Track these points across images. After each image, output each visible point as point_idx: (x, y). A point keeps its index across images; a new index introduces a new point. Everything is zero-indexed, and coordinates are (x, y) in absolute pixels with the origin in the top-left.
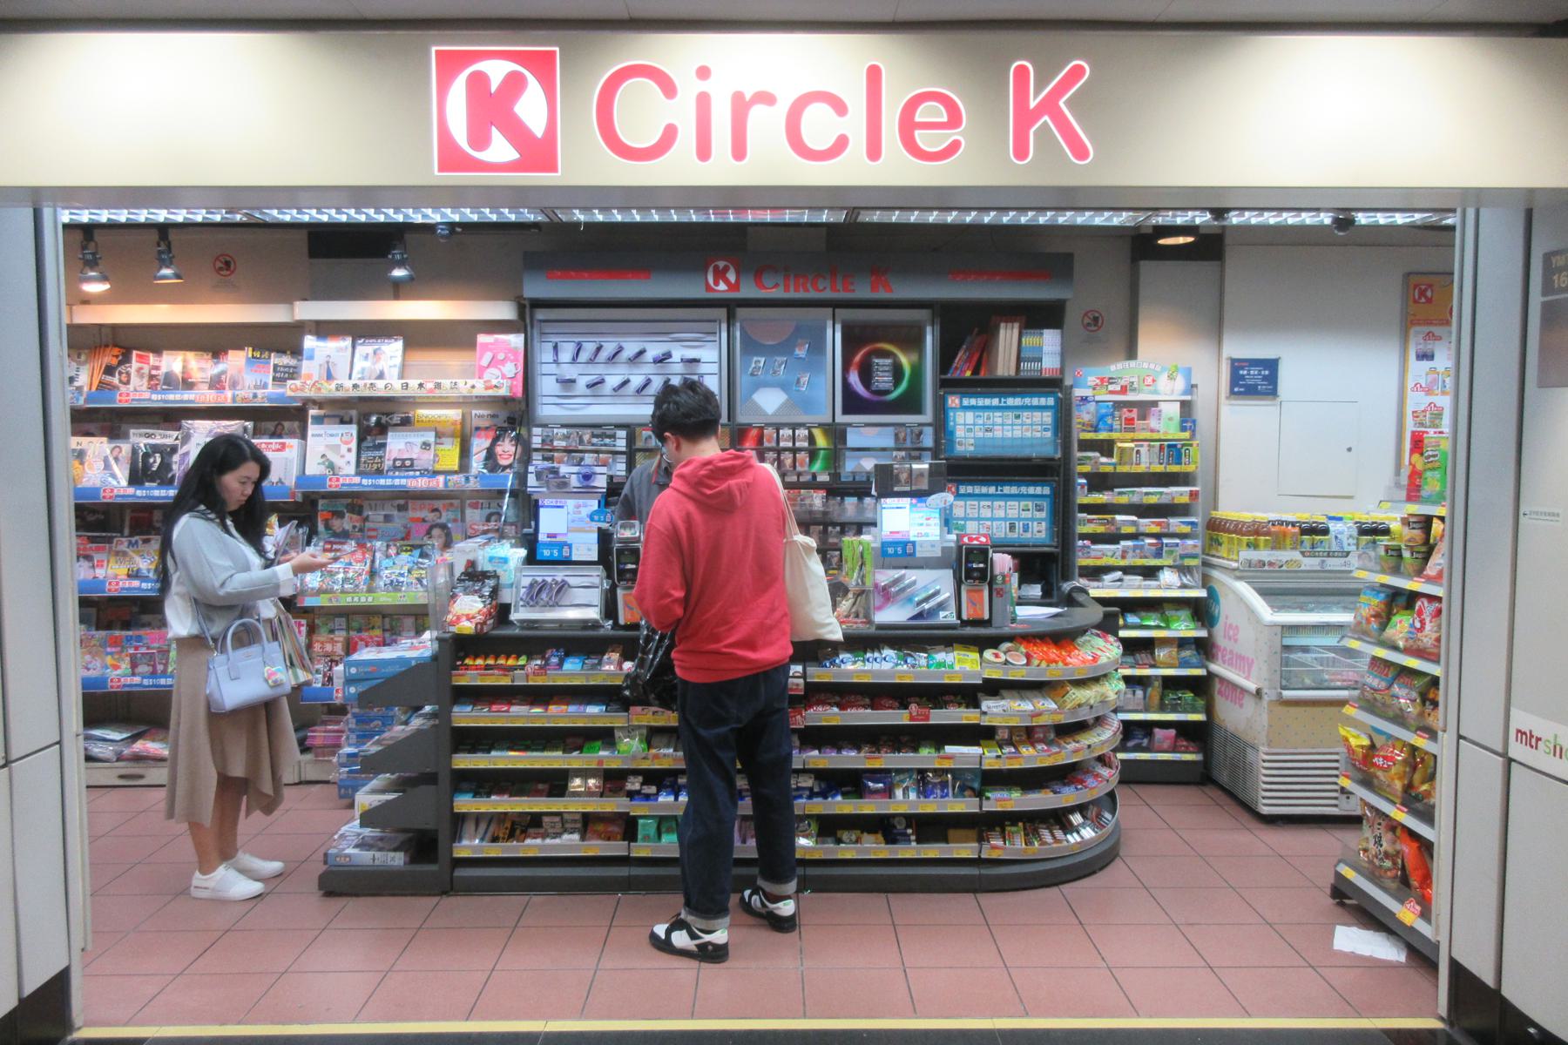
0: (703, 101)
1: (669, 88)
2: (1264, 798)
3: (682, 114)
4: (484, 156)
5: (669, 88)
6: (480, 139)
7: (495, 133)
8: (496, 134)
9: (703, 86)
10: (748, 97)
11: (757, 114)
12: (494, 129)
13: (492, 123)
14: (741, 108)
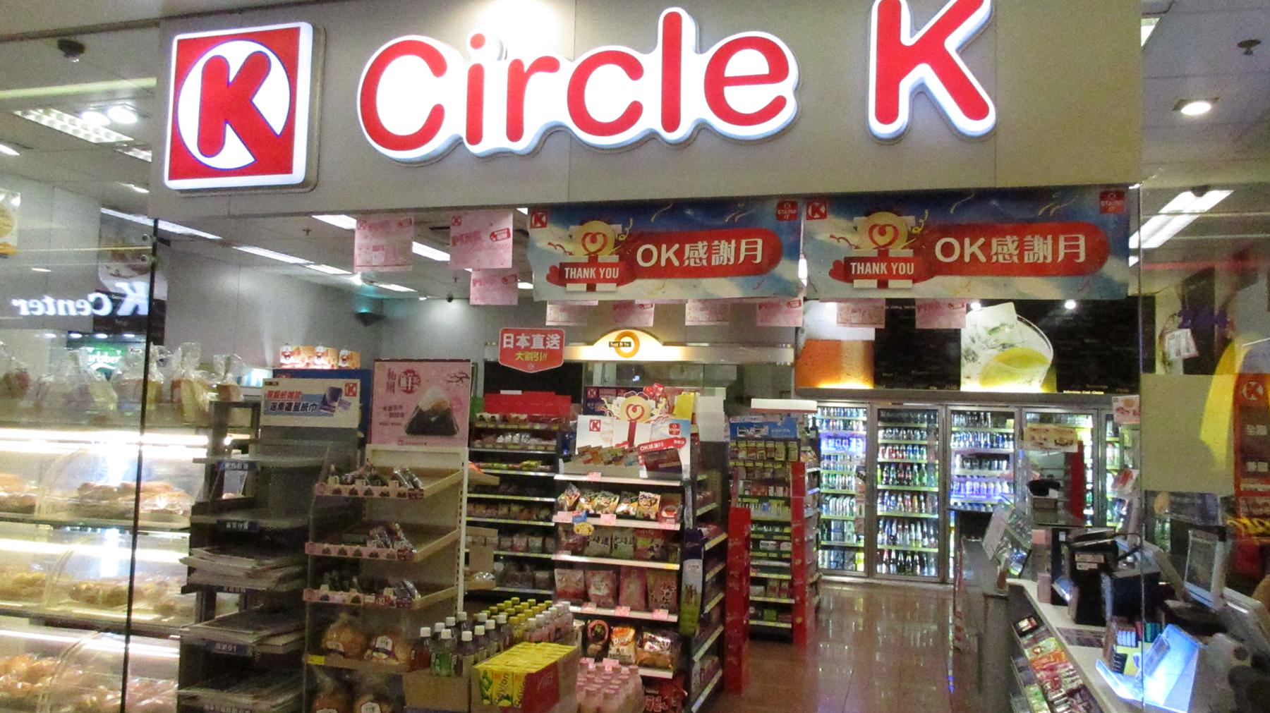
0: (476, 76)
1: (437, 65)
4: (214, 162)
5: (437, 65)
6: (211, 143)
7: (230, 135)
8: (230, 135)
9: (477, 57)
12: (228, 128)
13: (226, 122)
14: (518, 78)
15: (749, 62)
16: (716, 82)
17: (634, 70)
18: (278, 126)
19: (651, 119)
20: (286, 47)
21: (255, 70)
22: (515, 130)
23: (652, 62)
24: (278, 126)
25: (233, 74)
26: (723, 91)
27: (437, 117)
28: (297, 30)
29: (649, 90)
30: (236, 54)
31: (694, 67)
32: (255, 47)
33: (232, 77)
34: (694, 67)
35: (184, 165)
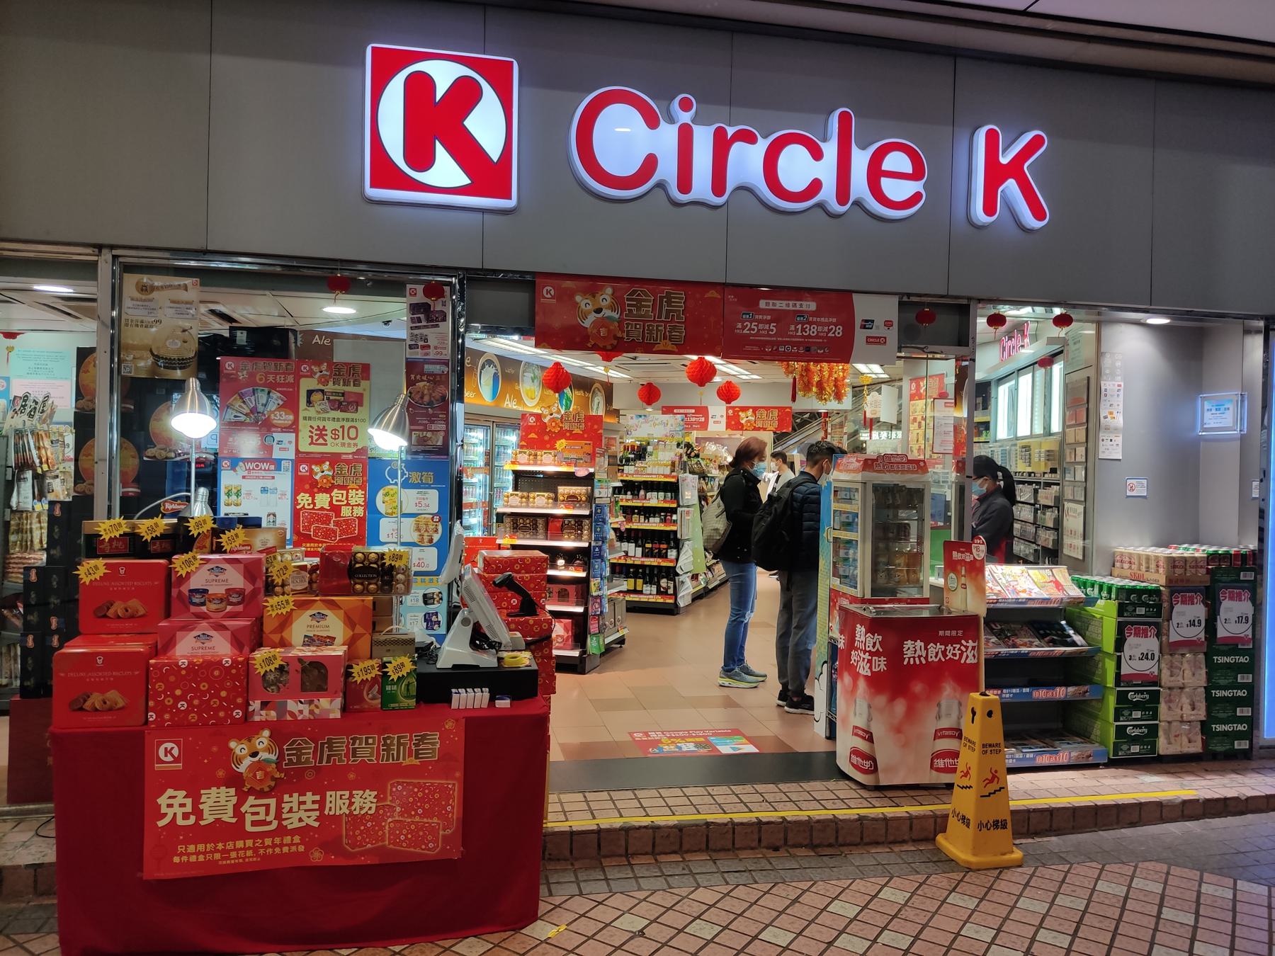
6: (420, 156)
7: (440, 151)
8: (440, 151)
10: (731, 131)
11: (738, 151)
15: (897, 161)
16: (875, 173)
17: (817, 154)
19: (828, 193)
21: (465, 95)
23: (830, 149)
24: (493, 149)
25: (440, 93)
26: (880, 181)
27: (650, 163)
29: (826, 170)
30: (444, 74)
31: (860, 160)
33: (439, 94)
34: (860, 160)
35: (385, 173)
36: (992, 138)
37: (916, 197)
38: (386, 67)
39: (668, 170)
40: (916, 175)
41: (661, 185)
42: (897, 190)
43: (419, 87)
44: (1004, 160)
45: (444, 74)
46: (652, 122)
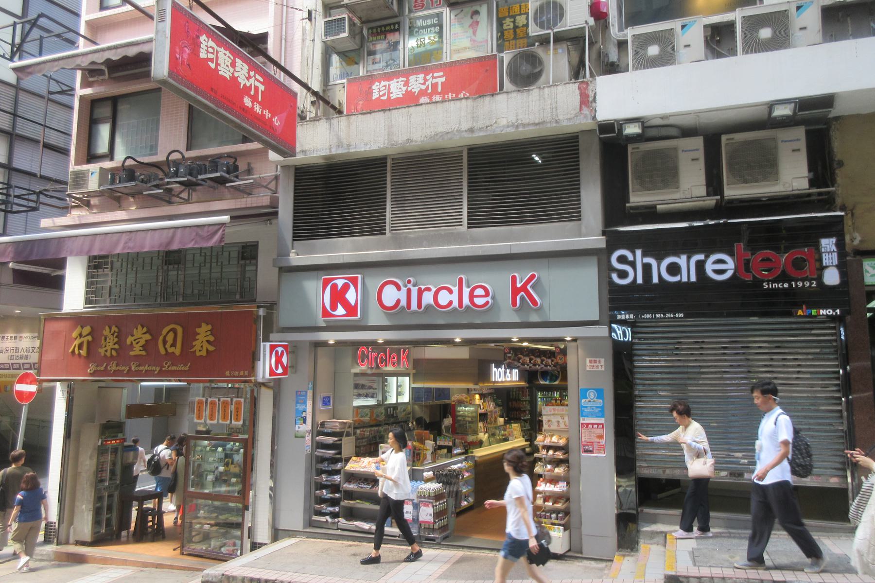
0: (409, 292)
2: (404, 66)
3: (402, 295)
6: (334, 307)
7: (339, 305)
8: (339, 305)
10: (423, 287)
14: (420, 293)
16: (472, 296)
17: (451, 292)
18: (353, 303)
19: (456, 304)
20: (354, 281)
21: (346, 287)
22: (419, 306)
23: (455, 289)
24: (352, 302)
25: (339, 288)
27: (398, 301)
28: (357, 277)
29: (455, 298)
30: (340, 283)
31: (466, 291)
32: (345, 281)
33: (339, 288)
34: (466, 291)
35: (325, 313)
36: (514, 278)
37: (487, 302)
38: (326, 283)
39: (404, 303)
40: (487, 294)
41: (403, 307)
42: (479, 301)
43: (335, 286)
44: (519, 285)
45: (340, 283)
46: (399, 288)
